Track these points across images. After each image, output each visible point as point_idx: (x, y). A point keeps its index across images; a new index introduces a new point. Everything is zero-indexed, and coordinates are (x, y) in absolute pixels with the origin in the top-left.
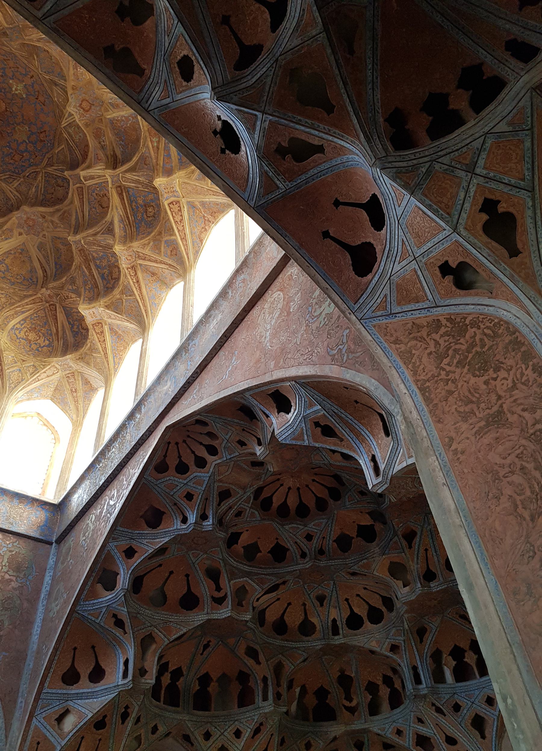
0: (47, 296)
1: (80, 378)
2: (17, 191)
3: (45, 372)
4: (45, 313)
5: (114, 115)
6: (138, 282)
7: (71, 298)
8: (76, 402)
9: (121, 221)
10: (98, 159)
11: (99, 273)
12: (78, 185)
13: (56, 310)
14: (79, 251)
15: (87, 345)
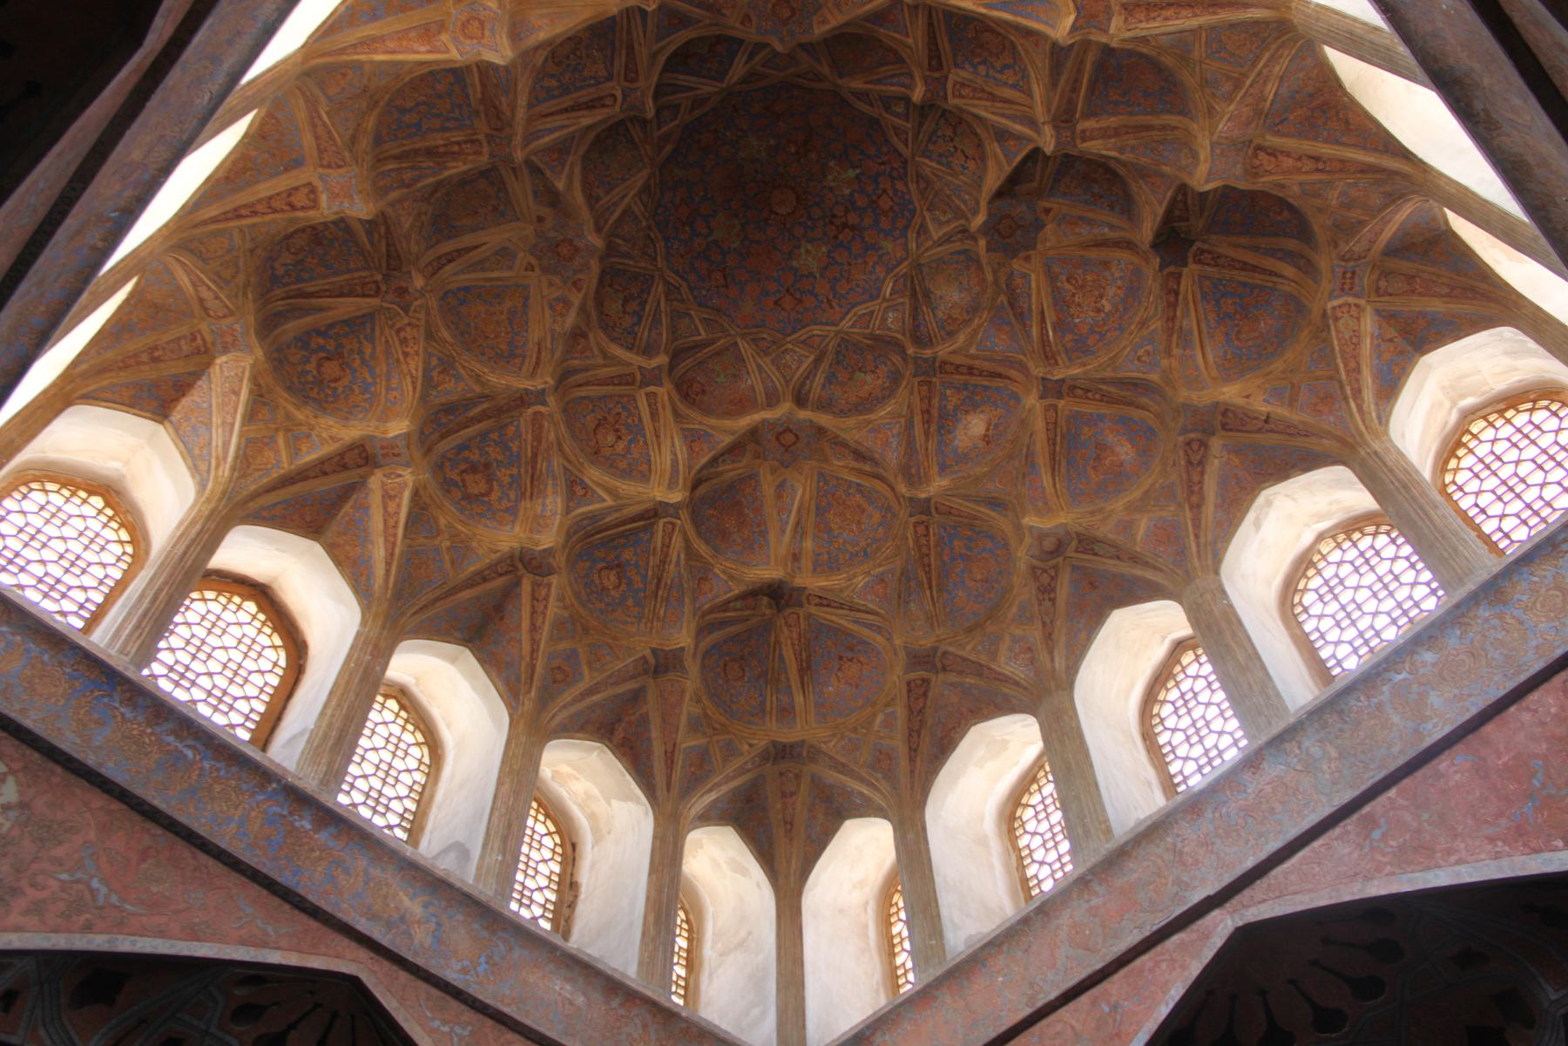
0: (403, 284)
1: (192, 369)
2: (624, 213)
3: (217, 298)
4: (357, 270)
5: (765, 486)
6: (485, 580)
7: (406, 354)
8: (125, 364)
9: (593, 517)
10: (693, 439)
11: (470, 439)
12: (639, 377)
13: (364, 296)
14: (521, 398)
15: (298, 409)
